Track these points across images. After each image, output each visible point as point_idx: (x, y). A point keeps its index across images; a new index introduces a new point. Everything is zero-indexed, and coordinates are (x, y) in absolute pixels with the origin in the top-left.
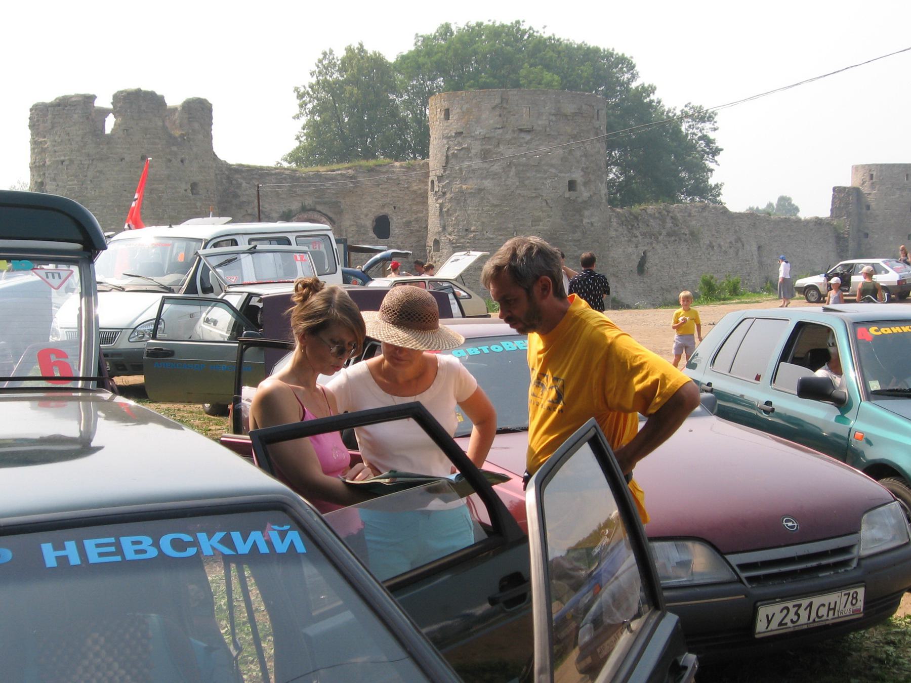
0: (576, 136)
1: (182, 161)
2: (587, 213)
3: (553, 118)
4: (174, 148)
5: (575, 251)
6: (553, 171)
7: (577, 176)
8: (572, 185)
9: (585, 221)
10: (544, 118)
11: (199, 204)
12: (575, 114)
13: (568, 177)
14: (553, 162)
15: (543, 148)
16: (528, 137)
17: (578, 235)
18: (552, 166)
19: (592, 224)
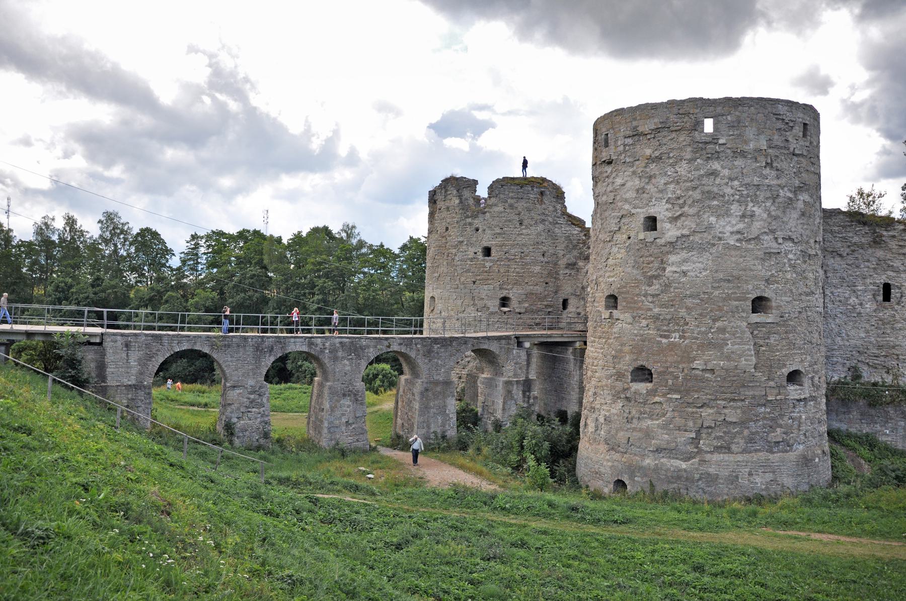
0: (659, 158)
1: (477, 230)
2: (673, 258)
3: (629, 141)
4: (469, 220)
5: (650, 310)
6: (627, 207)
7: (660, 210)
8: (652, 223)
9: (669, 269)
10: (619, 143)
11: (488, 264)
12: (657, 130)
13: (641, 214)
14: (628, 196)
15: (619, 181)
16: (609, 169)
17: (656, 287)
18: (626, 200)
19: (685, 273)
